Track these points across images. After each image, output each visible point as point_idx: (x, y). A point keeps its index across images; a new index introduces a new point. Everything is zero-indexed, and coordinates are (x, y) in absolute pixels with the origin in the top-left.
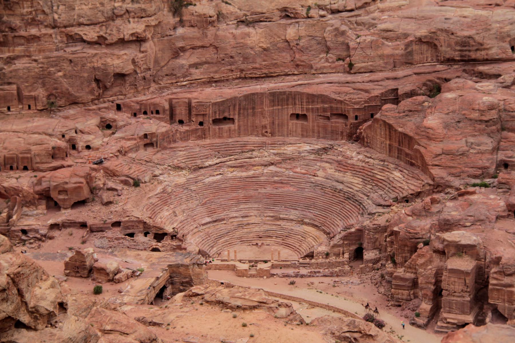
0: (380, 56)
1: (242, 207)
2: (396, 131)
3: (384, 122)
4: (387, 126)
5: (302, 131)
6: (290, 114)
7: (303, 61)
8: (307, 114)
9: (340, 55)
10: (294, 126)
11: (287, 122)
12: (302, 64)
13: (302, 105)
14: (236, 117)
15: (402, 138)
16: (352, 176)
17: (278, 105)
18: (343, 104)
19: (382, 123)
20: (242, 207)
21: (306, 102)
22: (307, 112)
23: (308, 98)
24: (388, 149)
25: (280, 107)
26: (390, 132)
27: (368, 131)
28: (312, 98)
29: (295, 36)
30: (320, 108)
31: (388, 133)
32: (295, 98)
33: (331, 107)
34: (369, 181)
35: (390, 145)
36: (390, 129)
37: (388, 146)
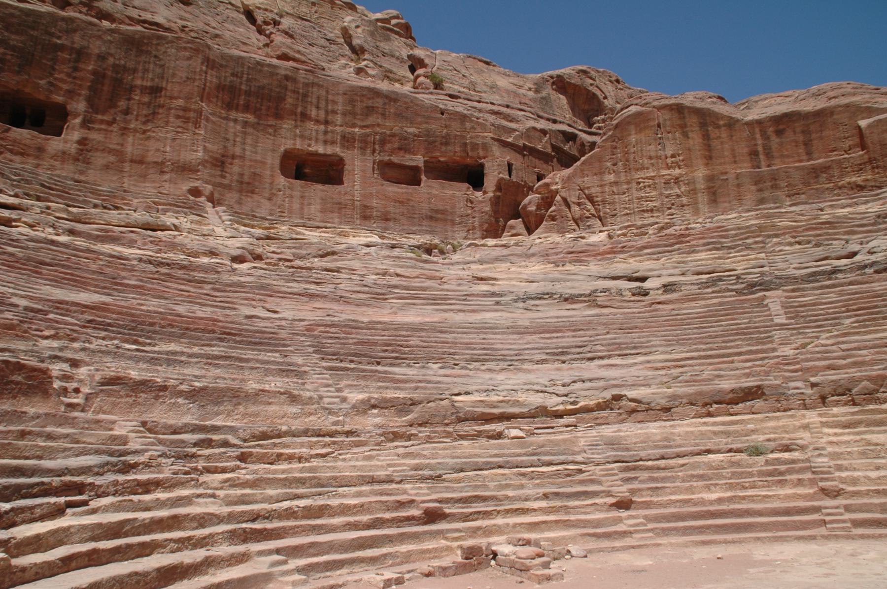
0: (492, 88)
1: (173, 347)
2: (732, 124)
3: (679, 109)
4: (692, 121)
5: (323, 211)
6: (282, 149)
7: (299, 52)
8: (346, 155)
9: (391, 72)
10: (297, 194)
11: (272, 176)
12: (297, 56)
13: (326, 123)
14: (80, 106)
15: (765, 136)
16: (650, 259)
17: (247, 108)
18: (468, 125)
19: (663, 117)
20: (173, 347)
21: (344, 114)
22: (343, 146)
23: (352, 102)
24: (703, 198)
25: (251, 118)
26: (706, 137)
27: (589, 181)
28: (364, 103)
29: (267, 4)
30: (393, 135)
31: (696, 139)
32: (305, 96)
33: (428, 133)
34: (762, 242)
35: (710, 179)
36: (703, 125)
37: (701, 185)
